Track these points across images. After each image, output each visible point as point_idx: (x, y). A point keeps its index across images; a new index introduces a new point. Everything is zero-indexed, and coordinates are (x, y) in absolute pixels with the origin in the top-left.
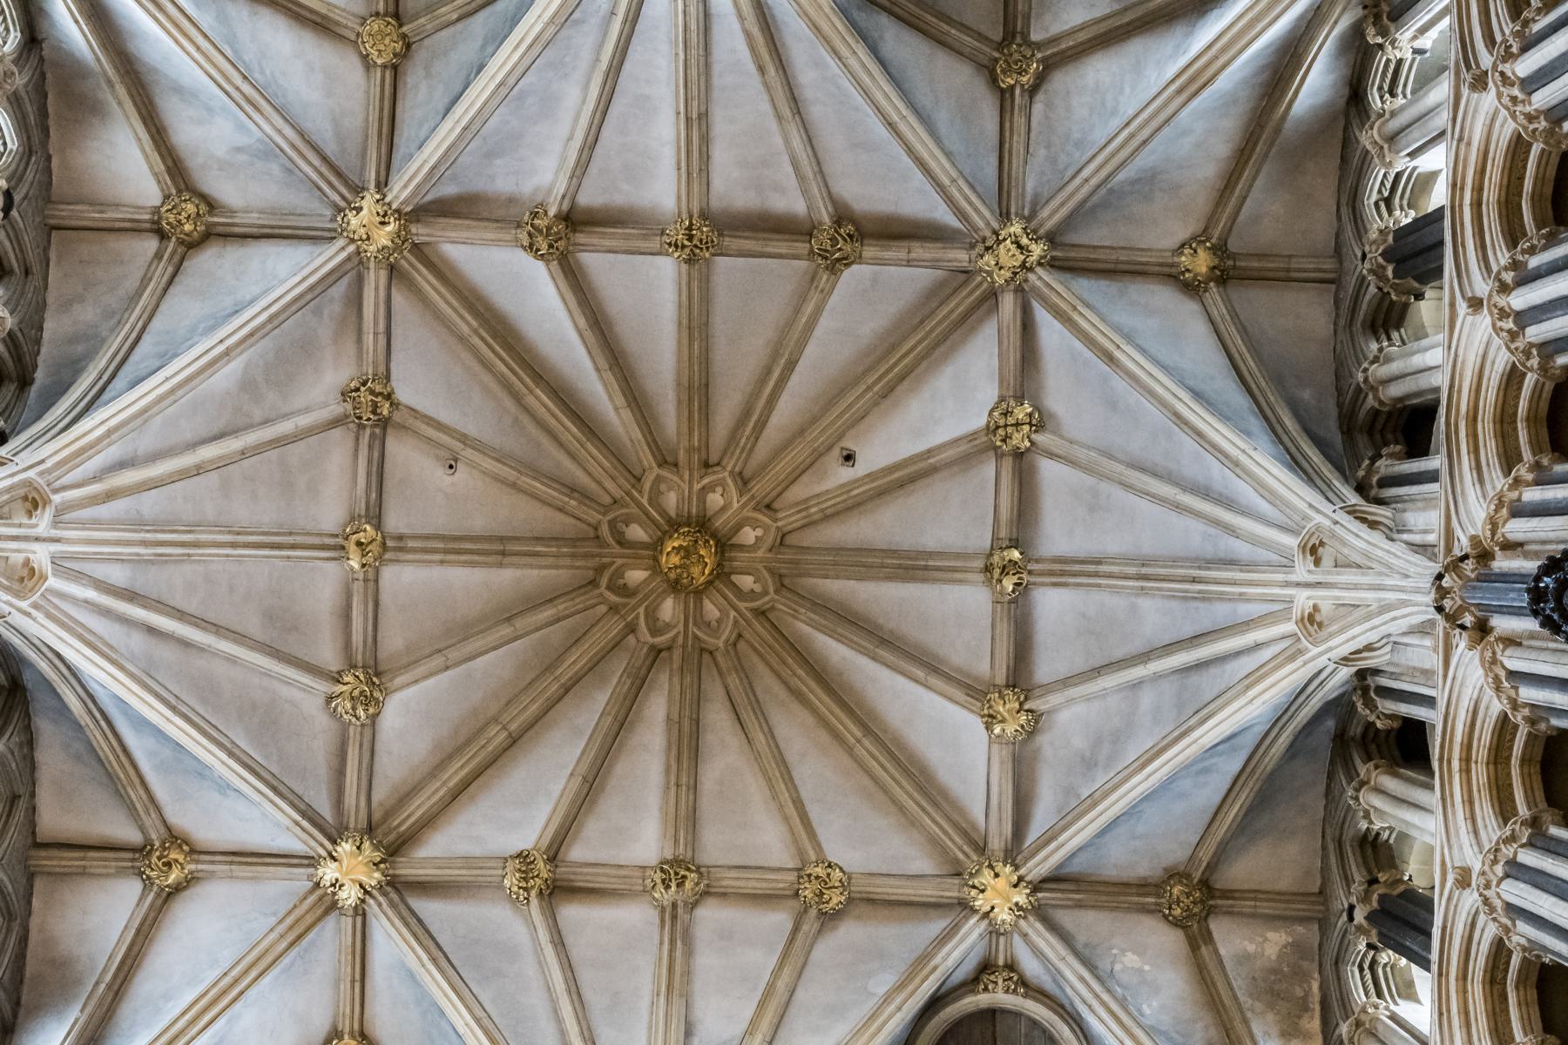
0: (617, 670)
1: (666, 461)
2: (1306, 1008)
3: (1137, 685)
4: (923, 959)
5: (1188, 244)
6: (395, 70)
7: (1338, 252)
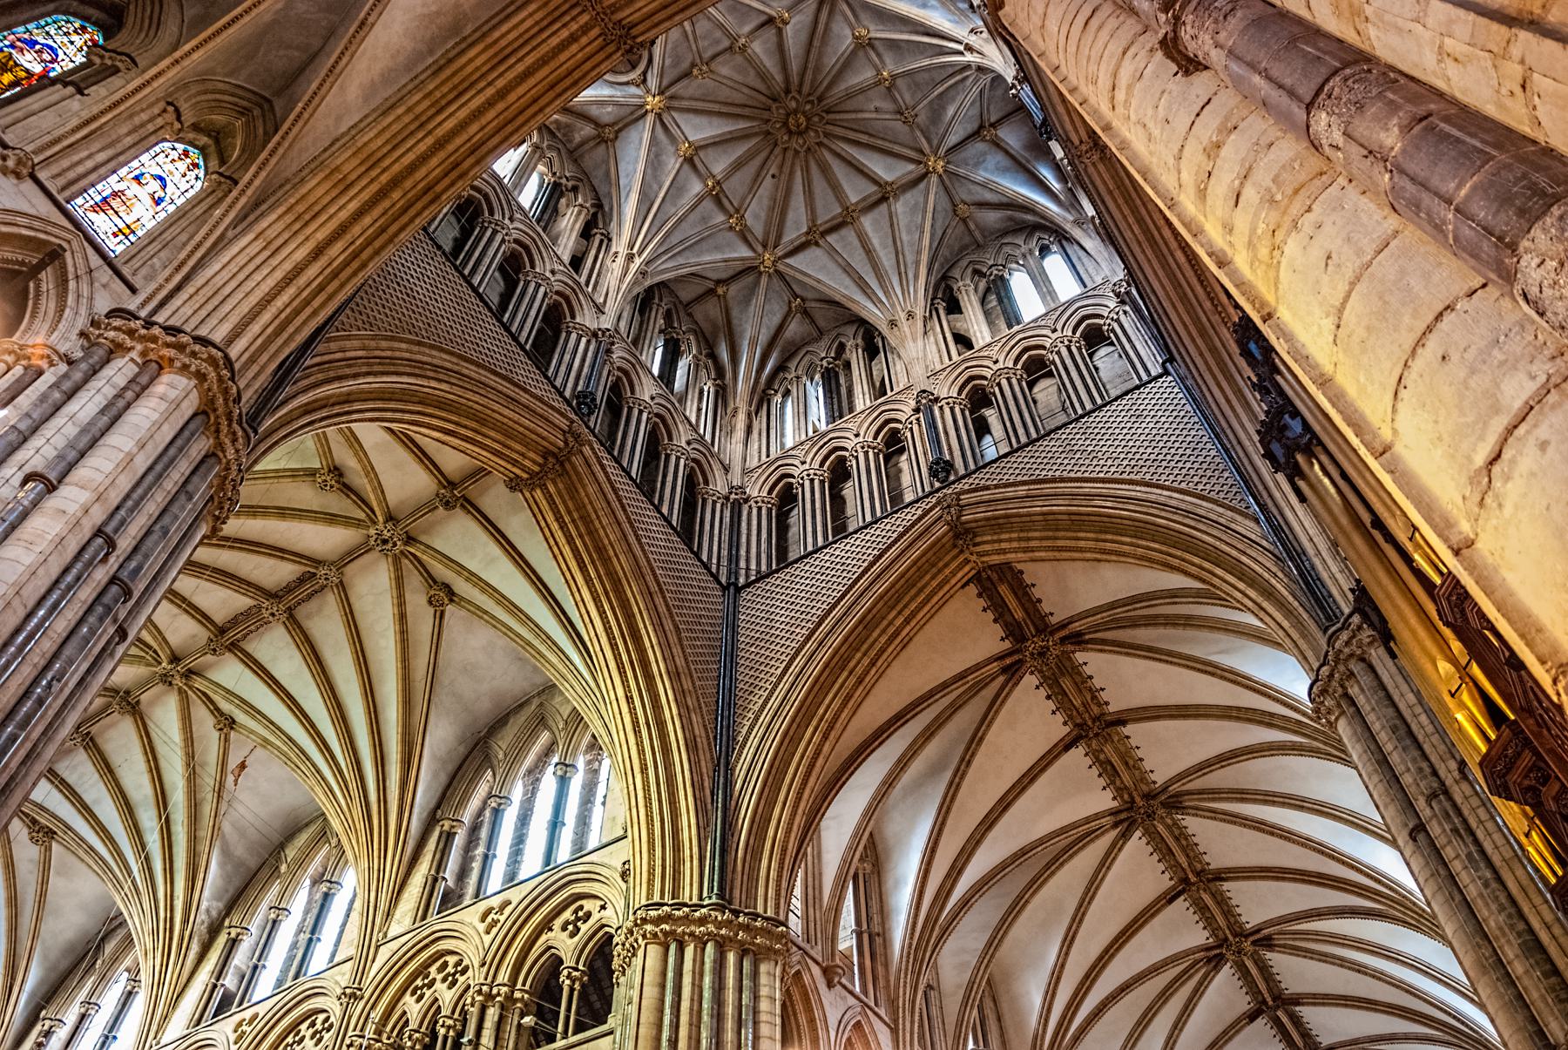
0: (795, 79)
1: (820, 144)
2: (558, 129)
3: (660, 188)
4: (661, 75)
5: (725, 293)
6: (955, 206)
7: (690, 315)
